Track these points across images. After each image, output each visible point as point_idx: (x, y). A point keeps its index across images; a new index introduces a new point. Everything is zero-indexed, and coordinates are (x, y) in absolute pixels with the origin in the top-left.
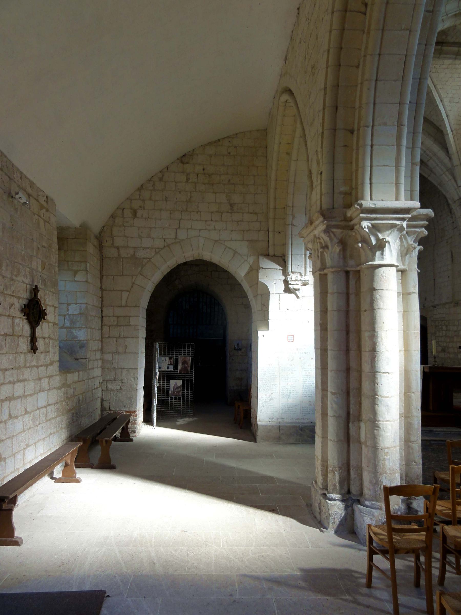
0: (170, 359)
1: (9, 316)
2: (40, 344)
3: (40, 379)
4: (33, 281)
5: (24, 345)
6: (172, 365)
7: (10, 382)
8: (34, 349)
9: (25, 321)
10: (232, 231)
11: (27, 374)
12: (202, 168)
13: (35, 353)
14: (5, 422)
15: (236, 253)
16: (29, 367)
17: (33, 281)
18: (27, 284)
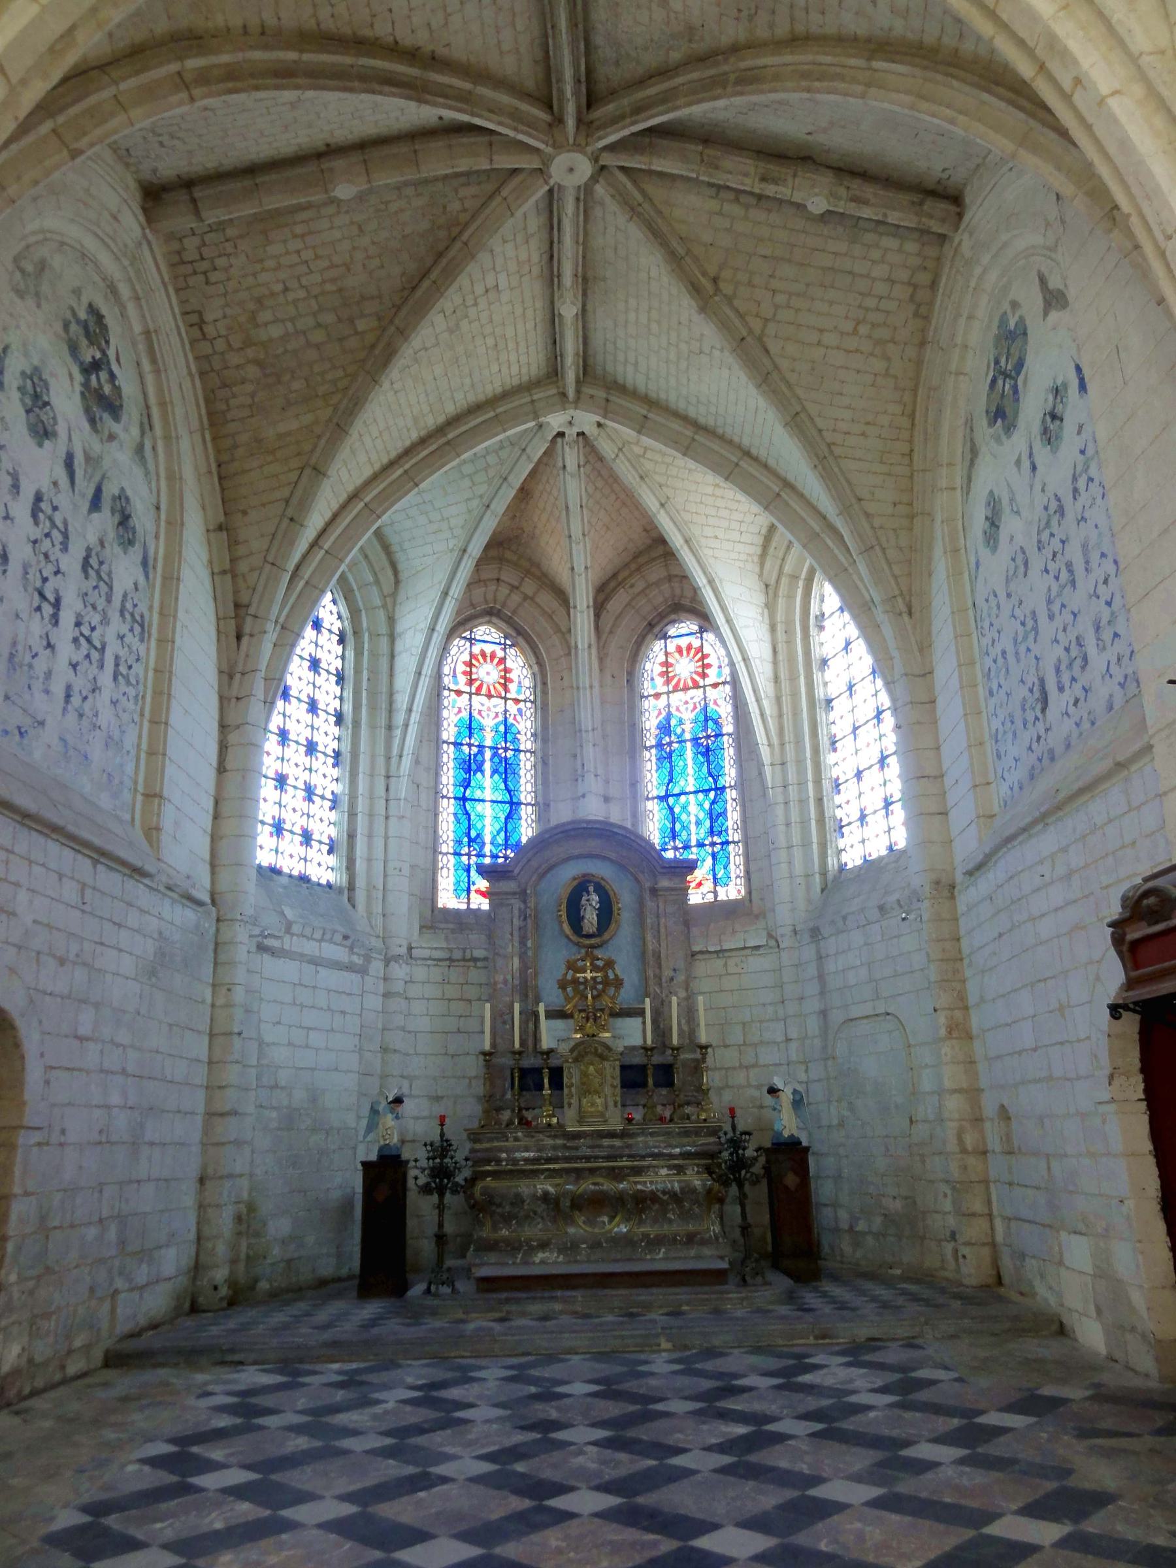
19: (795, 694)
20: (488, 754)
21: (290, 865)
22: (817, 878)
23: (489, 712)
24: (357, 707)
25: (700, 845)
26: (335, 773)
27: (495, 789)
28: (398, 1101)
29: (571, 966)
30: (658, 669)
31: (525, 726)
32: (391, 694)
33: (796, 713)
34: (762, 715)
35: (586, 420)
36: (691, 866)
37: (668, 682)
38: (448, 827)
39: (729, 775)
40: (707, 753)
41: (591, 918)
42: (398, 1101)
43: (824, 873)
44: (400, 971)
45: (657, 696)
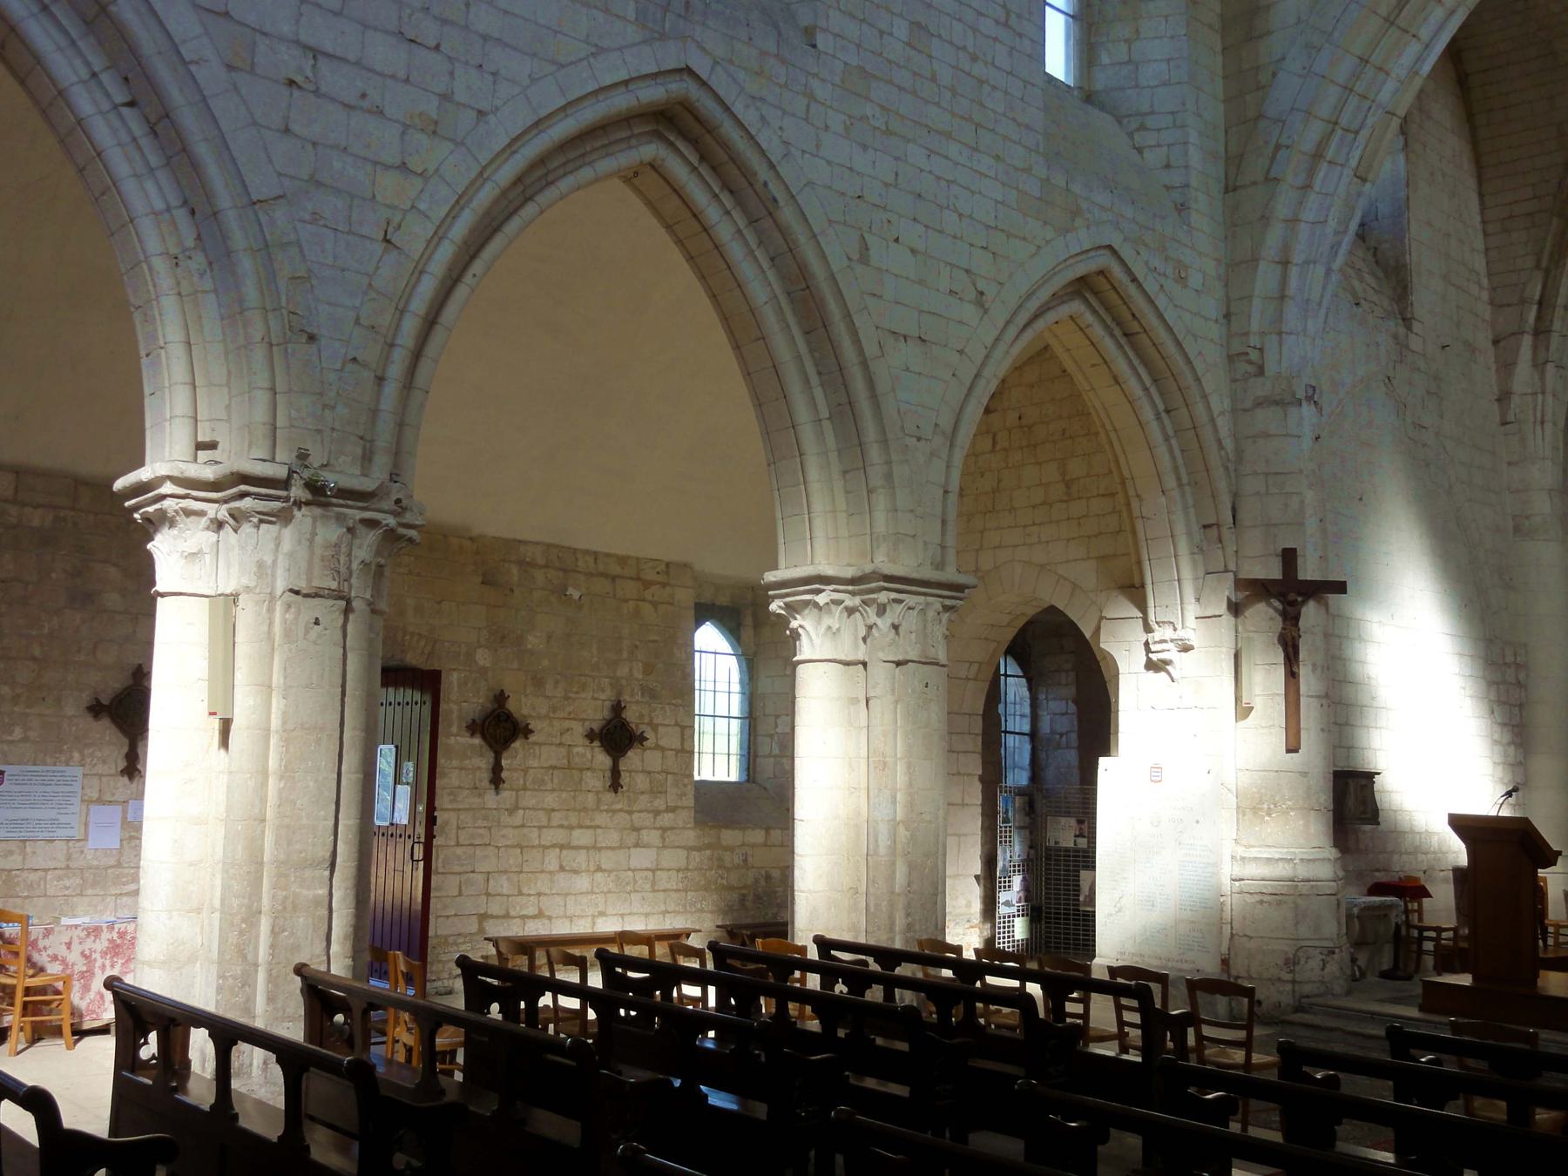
0: (1080, 822)
2: (625, 779)
3: (637, 830)
5: (596, 781)
6: (1084, 837)
7: (561, 826)
8: (615, 785)
10: (1068, 540)
11: (601, 819)
12: (1017, 415)
13: (616, 792)
14: (551, 873)
15: (1075, 586)
16: (607, 811)
18: (603, 701)
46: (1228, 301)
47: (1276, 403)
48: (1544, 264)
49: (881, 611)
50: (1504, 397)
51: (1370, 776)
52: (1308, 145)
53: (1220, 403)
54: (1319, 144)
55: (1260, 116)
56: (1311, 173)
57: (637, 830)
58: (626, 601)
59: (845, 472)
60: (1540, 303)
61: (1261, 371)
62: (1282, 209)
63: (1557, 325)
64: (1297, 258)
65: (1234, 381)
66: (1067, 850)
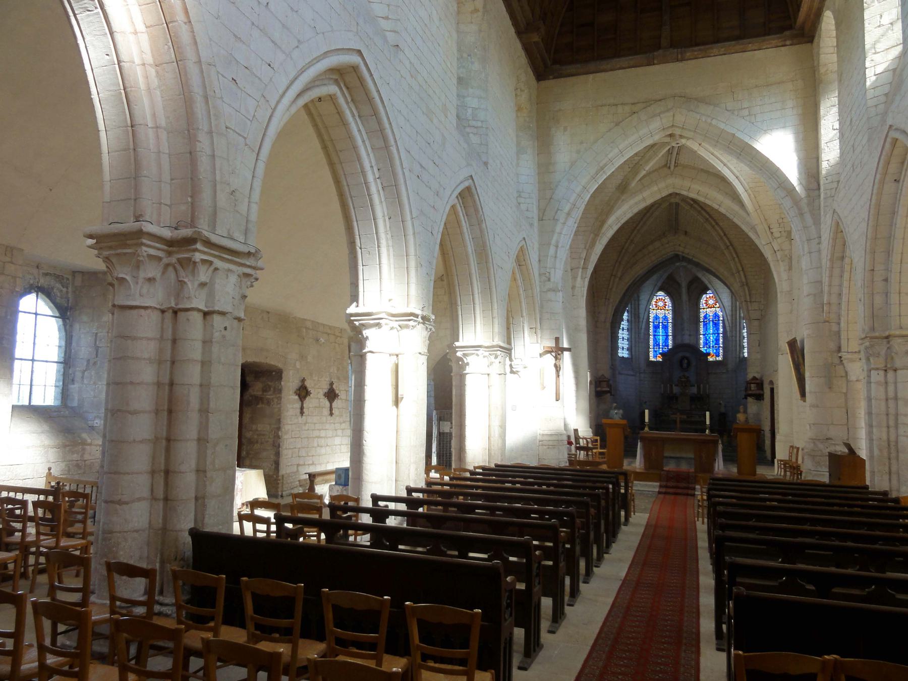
1: (317, 398)
2: (335, 411)
3: (336, 430)
4: (331, 379)
5: (326, 412)
7: (318, 429)
8: (331, 414)
9: (326, 400)
11: (328, 426)
17: (331, 379)
19: (736, 315)
20: (661, 324)
21: (620, 355)
22: (738, 359)
23: (661, 314)
24: (631, 317)
25: (713, 347)
26: (627, 333)
27: (662, 332)
28: (646, 402)
29: (680, 378)
30: (704, 302)
31: (670, 316)
32: (639, 314)
33: (736, 319)
34: (728, 320)
35: (684, 264)
36: (709, 354)
37: (707, 305)
38: (651, 342)
39: (721, 330)
40: (716, 325)
41: (685, 365)
42: (646, 402)
43: (740, 355)
44: (642, 375)
45: (704, 309)
46: (539, 256)
47: (554, 291)
48: (587, 248)
49: (496, 357)
50: (573, 287)
51: (576, 409)
52: (567, 209)
53: (538, 290)
54: (569, 212)
55: (551, 198)
56: (566, 219)
57: (336, 430)
58: (332, 343)
59: (483, 311)
60: (585, 259)
61: (549, 280)
62: (558, 229)
63: (589, 267)
64: (560, 246)
65: (540, 282)
66: (447, 433)
